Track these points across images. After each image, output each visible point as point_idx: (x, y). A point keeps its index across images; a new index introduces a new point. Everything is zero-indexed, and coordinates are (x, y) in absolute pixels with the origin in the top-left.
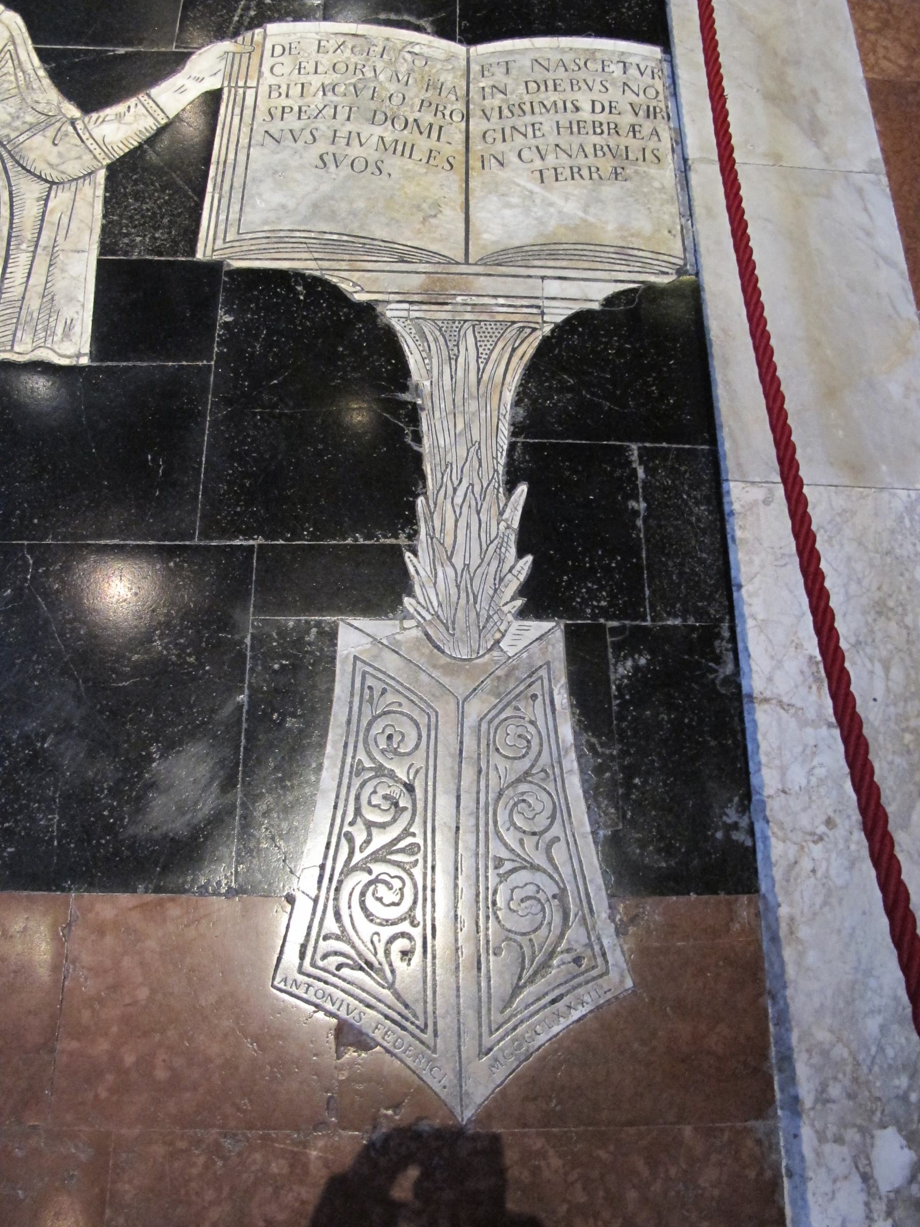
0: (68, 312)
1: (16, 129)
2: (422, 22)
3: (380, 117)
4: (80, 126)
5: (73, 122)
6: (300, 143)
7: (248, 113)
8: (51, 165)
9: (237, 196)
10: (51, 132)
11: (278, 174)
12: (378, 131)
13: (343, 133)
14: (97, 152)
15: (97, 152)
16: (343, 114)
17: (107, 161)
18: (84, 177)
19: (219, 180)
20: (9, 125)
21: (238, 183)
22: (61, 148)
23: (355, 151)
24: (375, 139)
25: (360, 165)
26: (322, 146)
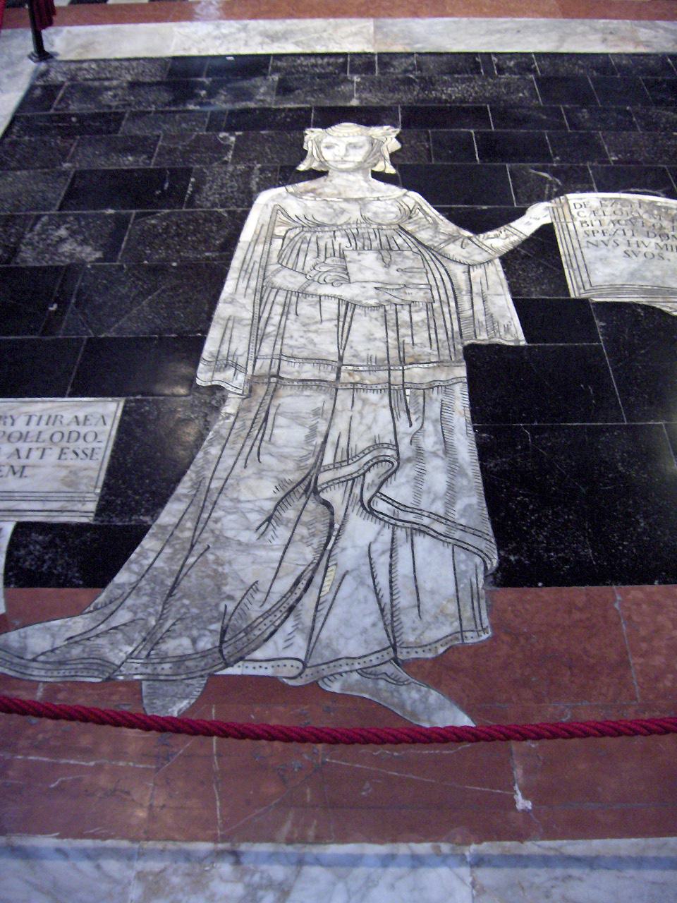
0: (504, 322)
1: (436, 242)
2: (657, 192)
3: (651, 234)
4: (474, 240)
5: (469, 238)
6: (610, 247)
7: (573, 233)
8: (465, 257)
9: (583, 270)
10: (458, 243)
11: (603, 260)
12: (653, 241)
13: (633, 240)
14: (490, 251)
15: (490, 251)
16: (629, 233)
17: (497, 255)
18: (487, 262)
19: (569, 262)
20: (431, 240)
21: (581, 264)
22: (468, 249)
23: (643, 249)
24: (653, 245)
25: (649, 256)
26: (624, 248)
